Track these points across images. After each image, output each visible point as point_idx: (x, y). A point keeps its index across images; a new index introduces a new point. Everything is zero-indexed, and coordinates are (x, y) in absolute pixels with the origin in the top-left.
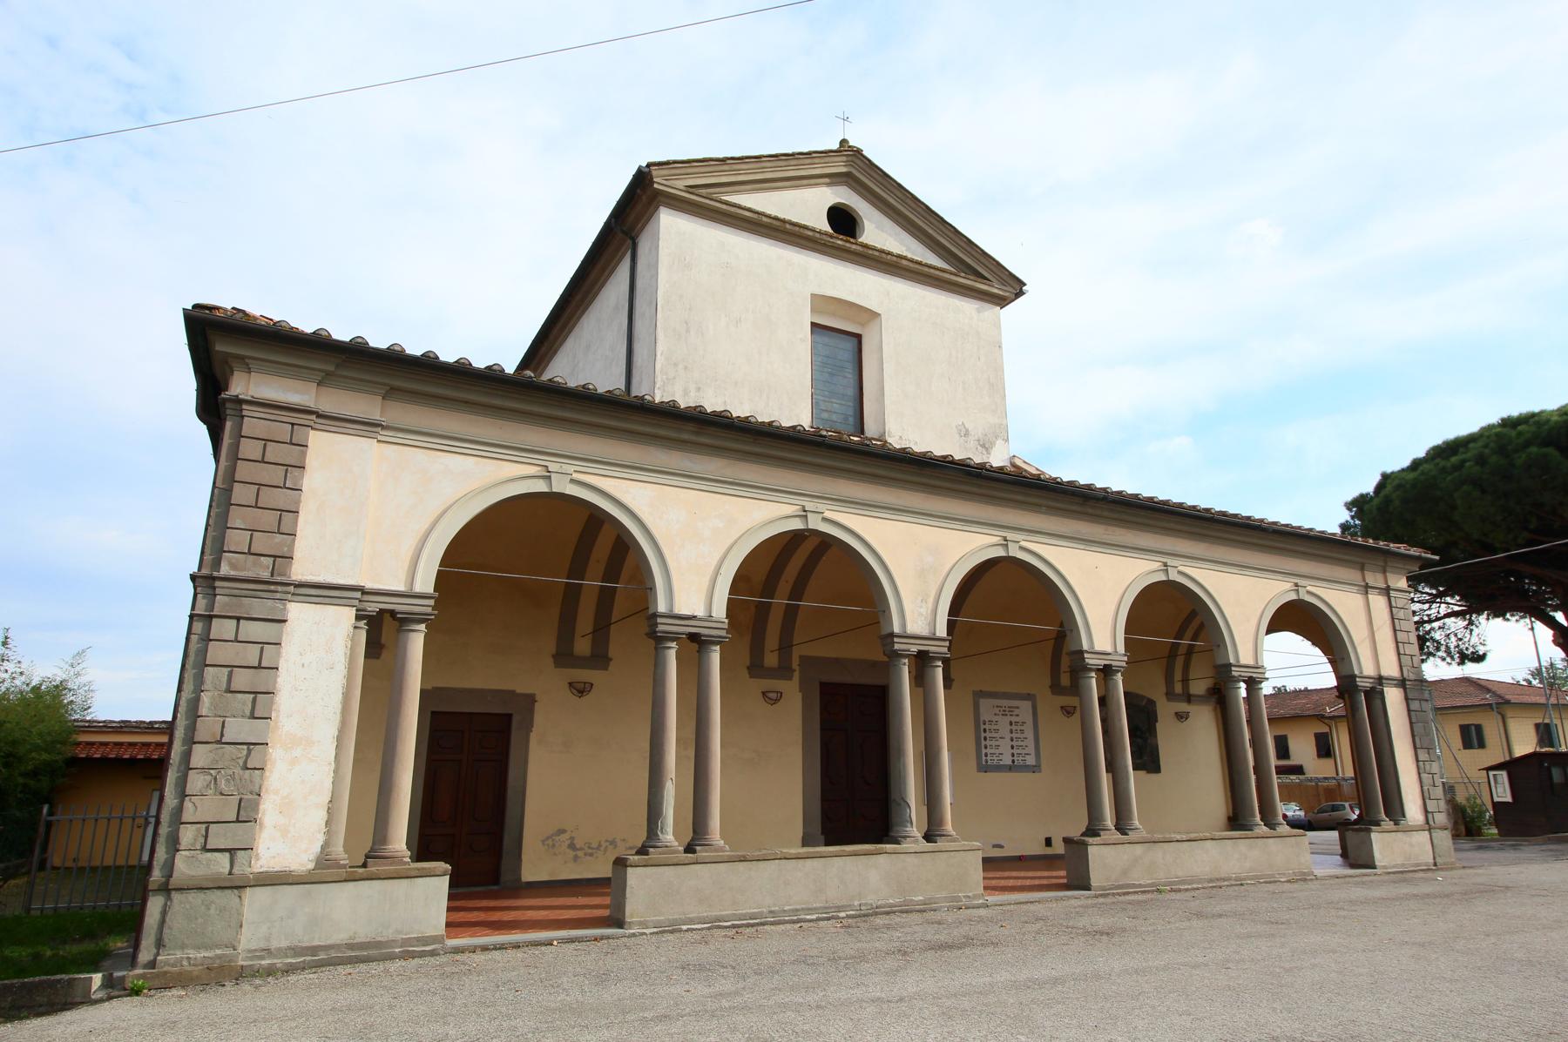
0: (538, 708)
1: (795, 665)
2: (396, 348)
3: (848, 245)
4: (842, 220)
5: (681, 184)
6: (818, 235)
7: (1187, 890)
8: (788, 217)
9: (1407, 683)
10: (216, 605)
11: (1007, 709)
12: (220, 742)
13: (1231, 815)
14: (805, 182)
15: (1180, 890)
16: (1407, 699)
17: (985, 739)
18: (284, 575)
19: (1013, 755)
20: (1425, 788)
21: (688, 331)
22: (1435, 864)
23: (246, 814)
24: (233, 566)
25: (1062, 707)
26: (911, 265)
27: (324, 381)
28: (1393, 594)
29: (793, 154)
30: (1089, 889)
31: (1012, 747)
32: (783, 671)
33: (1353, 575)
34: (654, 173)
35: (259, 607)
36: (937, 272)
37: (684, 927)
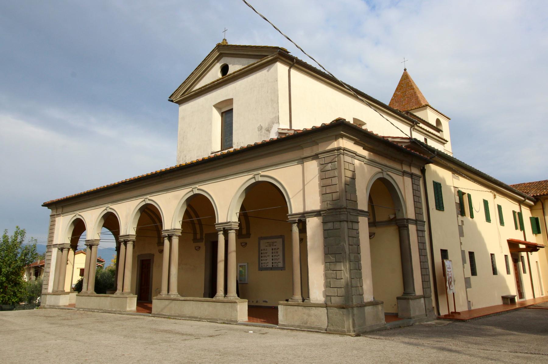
2: (249, 146)
17: (262, 257)
19: (273, 263)
29: (201, 64)
31: (273, 260)
32: (201, 240)
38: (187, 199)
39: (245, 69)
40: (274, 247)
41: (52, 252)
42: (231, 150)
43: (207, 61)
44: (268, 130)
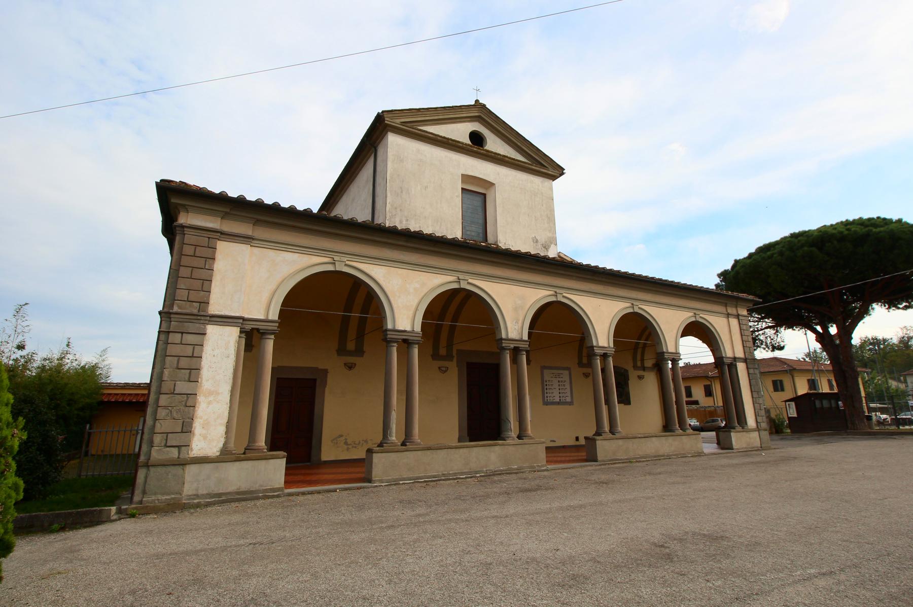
0: (329, 376)
1: (454, 354)
3: (479, 150)
4: (477, 139)
5: (398, 121)
6: (464, 146)
7: (643, 461)
8: (450, 137)
9: (748, 360)
10: (171, 326)
11: (557, 375)
12: (173, 393)
13: (664, 424)
14: (458, 120)
15: (640, 461)
16: (747, 368)
17: (547, 389)
18: (205, 311)
19: (560, 397)
20: (756, 411)
21: (402, 192)
22: (761, 447)
23: (187, 428)
24: (180, 307)
25: (583, 374)
26: (510, 160)
27: (225, 216)
28: (740, 318)
30: (597, 462)
31: (560, 393)
32: (449, 357)
33: (721, 309)
34: (385, 116)
35: (192, 327)
36: (522, 164)
37: (401, 482)
40: (560, 379)
41: (206, 334)
43: (460, 110)
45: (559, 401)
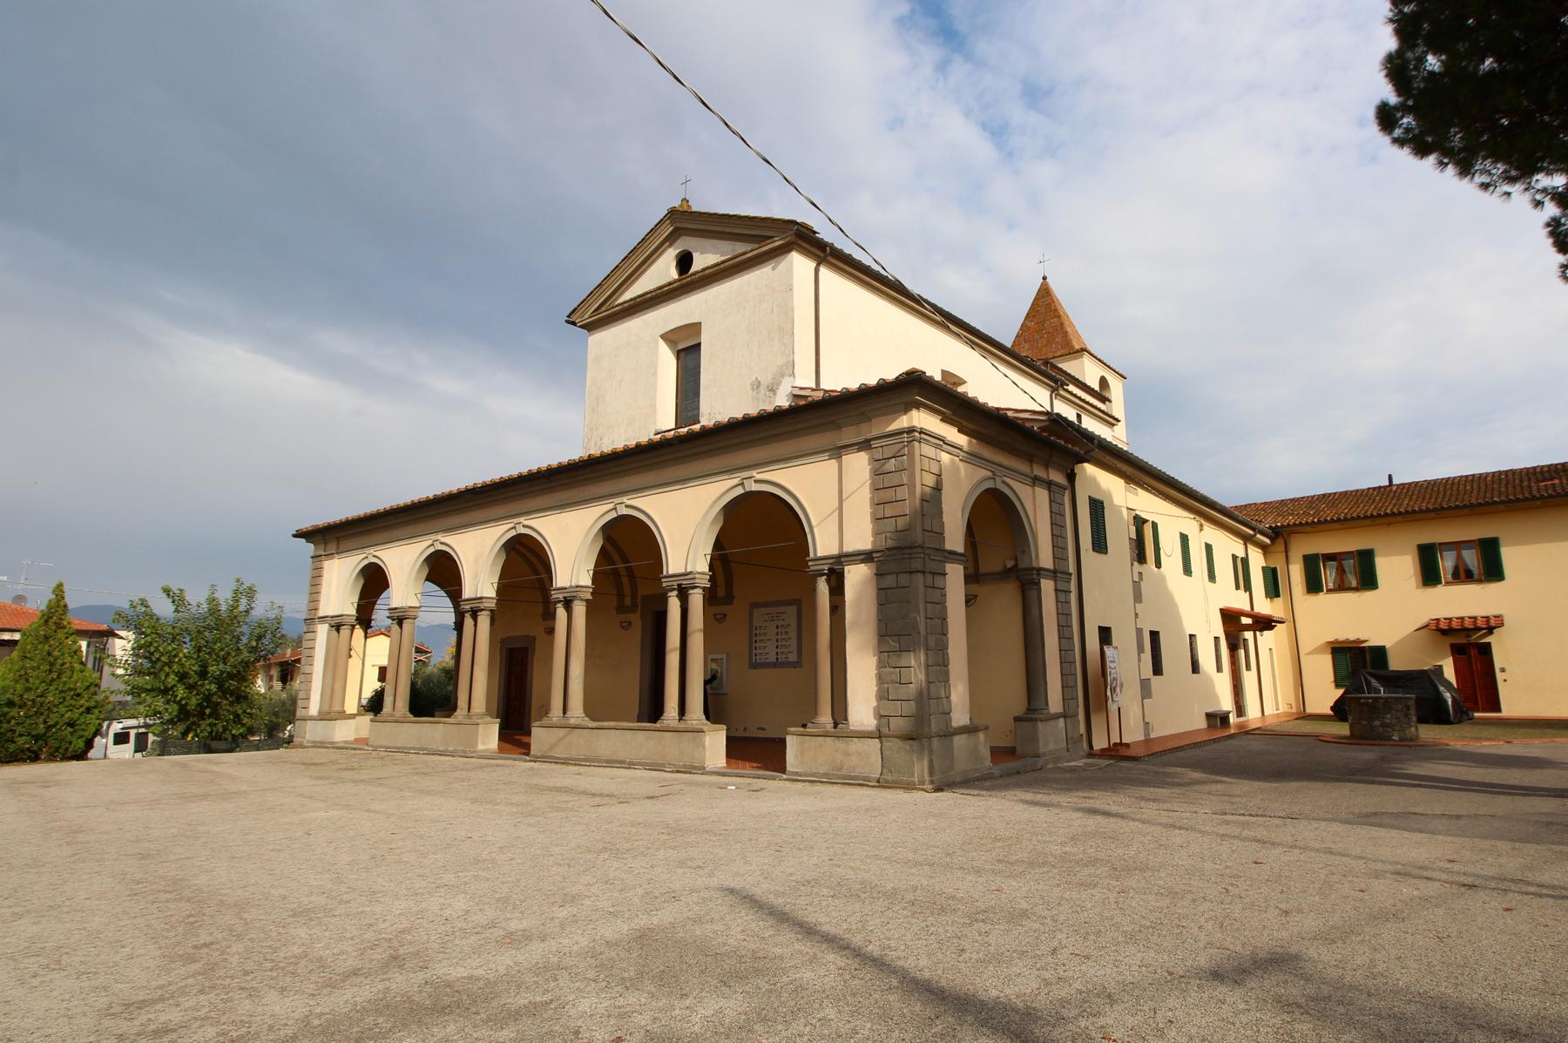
2: (731, 420)
14: (654, 257)
19: (777, 654)
29: (635, 248)
31: (777, 647)
38: (727, 504)
39: (727, 264)
42: (697, 427)
43: (648, 242)
44: (773, 390)
45: (774, 660)
